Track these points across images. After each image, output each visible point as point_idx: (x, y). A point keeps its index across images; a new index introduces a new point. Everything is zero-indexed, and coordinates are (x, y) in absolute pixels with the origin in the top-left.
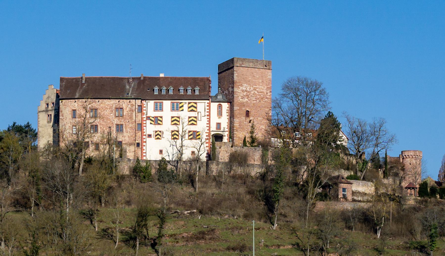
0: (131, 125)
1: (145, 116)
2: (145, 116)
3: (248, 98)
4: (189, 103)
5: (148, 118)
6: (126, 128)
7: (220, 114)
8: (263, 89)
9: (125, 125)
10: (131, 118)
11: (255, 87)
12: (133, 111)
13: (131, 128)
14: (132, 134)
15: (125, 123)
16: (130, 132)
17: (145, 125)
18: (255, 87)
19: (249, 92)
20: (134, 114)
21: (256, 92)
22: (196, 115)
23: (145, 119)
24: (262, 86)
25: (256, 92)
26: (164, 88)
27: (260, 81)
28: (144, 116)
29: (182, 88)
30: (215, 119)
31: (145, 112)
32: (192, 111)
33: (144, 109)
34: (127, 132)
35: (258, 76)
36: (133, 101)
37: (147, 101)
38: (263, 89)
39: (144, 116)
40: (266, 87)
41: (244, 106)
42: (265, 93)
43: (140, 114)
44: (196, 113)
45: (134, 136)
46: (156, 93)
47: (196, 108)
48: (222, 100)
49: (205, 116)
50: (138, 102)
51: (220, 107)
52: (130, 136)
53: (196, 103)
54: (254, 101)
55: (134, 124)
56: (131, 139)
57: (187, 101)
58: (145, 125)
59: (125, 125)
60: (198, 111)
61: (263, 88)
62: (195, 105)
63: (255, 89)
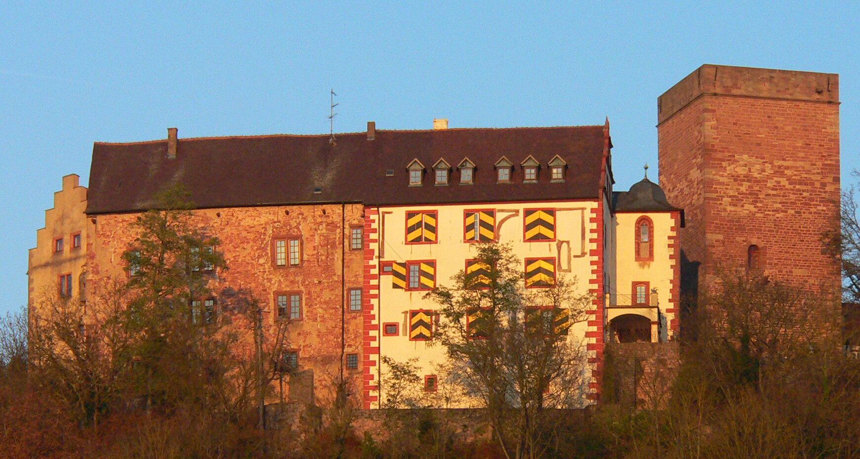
0: (326, 295)
1: (375, 262)
2: (375, 262)
3: (754, 203)
4: (528, 212)
5: (385, 267)
6: (310, 306)
7: (644, 253)
8: (808, 172)
9: (309, 293)
10: (328, 269)
11: (781, 163)
12: (334, 246)
13: (325, 302)
14: (331, 324)
15: (306, 286)
16: (324, 320)
17: (373, 292)
18: (781, 163)
19: (757, 181)
20: (338, 255)
21: (784, 182)
22: (554, 254)
23: (375, 271)
24: (803, 159)
25: (784, 182)
26: (443, 166)
27: (800, 144)
28: (371, 263)
29: (504, 164)
30: (627, 270)
31: (374, 246)
32: (539, 238)
33: (373, 236)
34: (315, 320)
35: (789, 128)
36: (335, 211)
37: (381, 210)
38: (808, 172)
39: (371, 263)
40: (819, 164)
41: (741, 229)
42: (818, 185)
43: (357, 258)
44: (554, 245)
45: (338, 331)
46: (415, 178)
47: (552, 227)
48: (652, 203)
49: (583, 254)
50: (354, 212)
51: (644, 228)
52: (324, 330)
53: (551, 212)
54: (777, 211)
55: (338, 291)
56: (328, 341)
57: (521, 207)
58: (373, 292)
59: (309, 293)
60: (560, 237)
61: (807, 166)
62: (549, 219)
63: (779, 171)
